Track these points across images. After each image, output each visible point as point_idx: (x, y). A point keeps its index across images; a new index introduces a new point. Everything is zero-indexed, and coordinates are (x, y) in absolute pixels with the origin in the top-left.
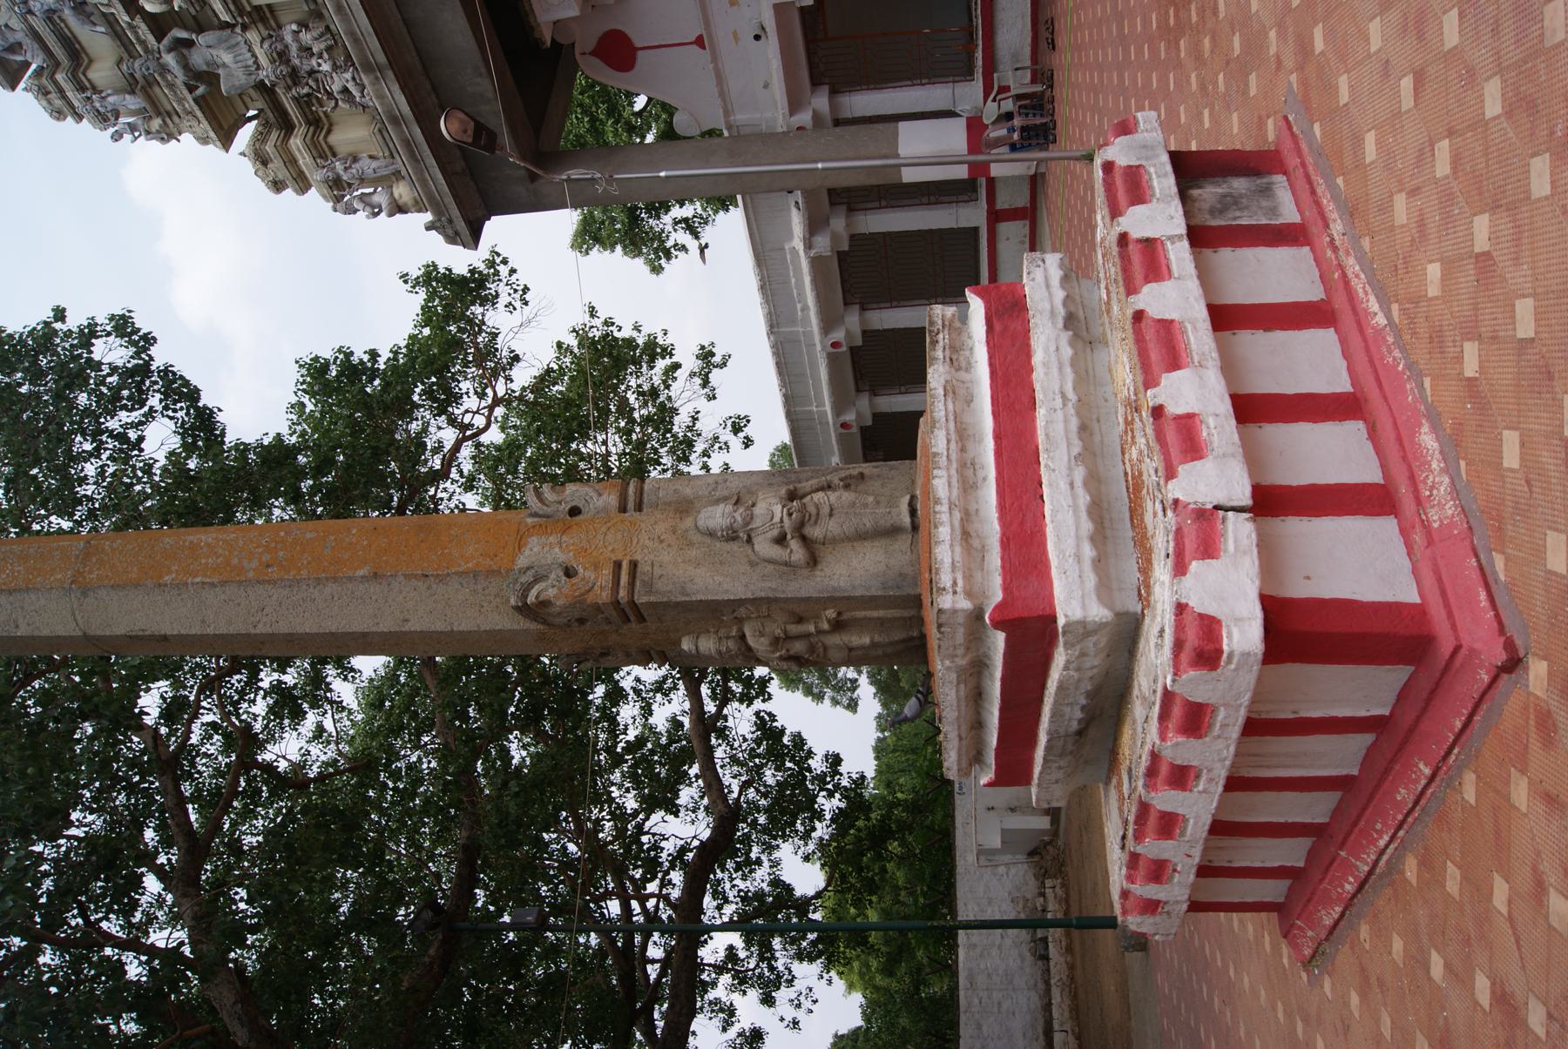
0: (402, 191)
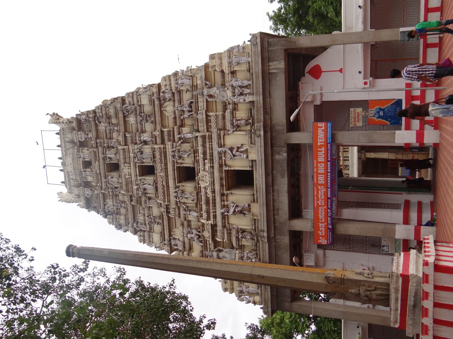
0: (257, 298)
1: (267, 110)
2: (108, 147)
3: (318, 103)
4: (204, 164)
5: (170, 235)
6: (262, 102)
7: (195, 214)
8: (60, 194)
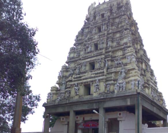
1: (111, 99)
2: (107, 26)
4: (93, 74)
5: (72, 62)
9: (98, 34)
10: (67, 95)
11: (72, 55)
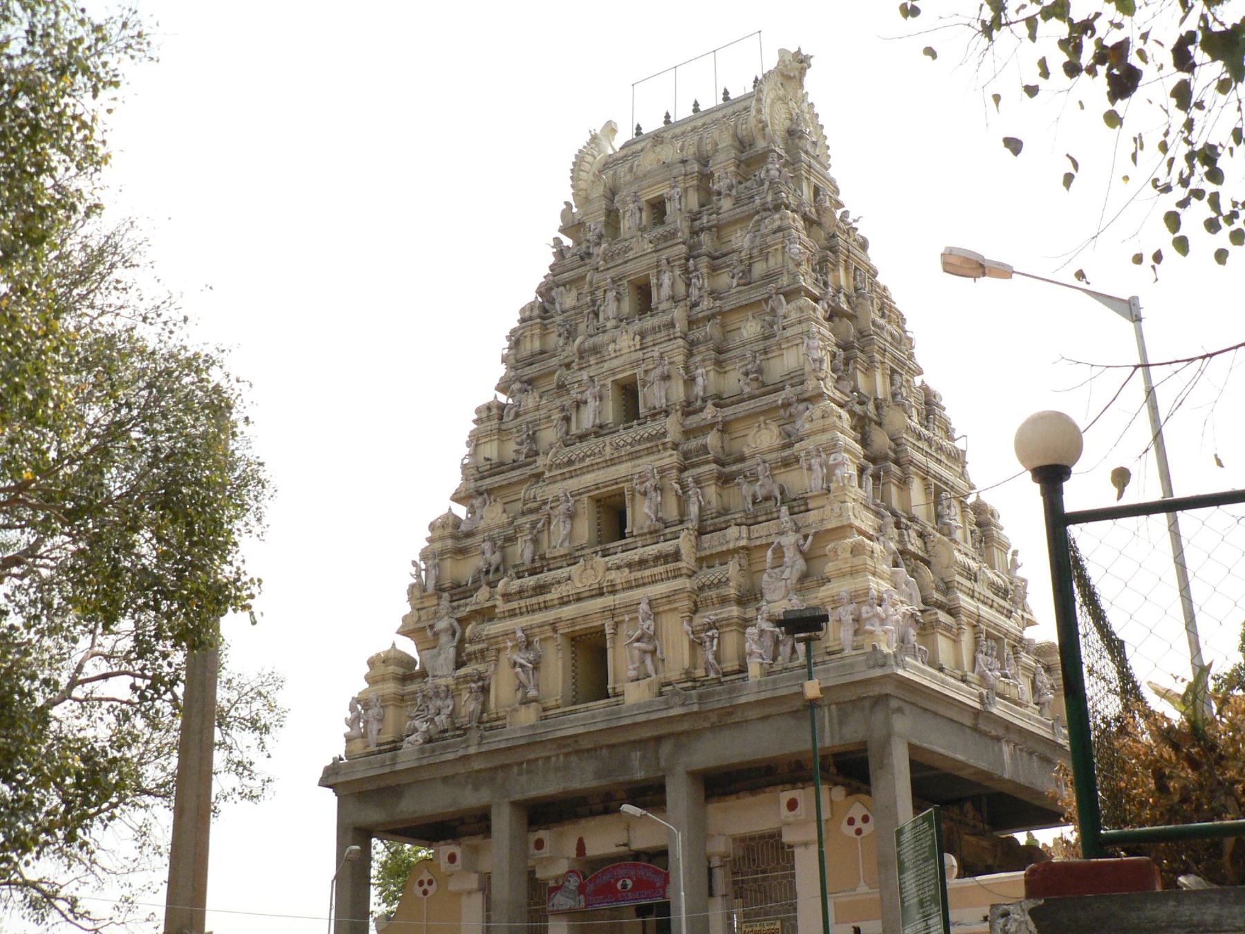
1: (728, 719)
2: (686, 271)
3: (786, 838)
5: (489, 492)
6: (743, 700)
7: (528, 555)
8: (611, 129)
9: (637, 326)
10: (469, 705)
11: (491, 450)
